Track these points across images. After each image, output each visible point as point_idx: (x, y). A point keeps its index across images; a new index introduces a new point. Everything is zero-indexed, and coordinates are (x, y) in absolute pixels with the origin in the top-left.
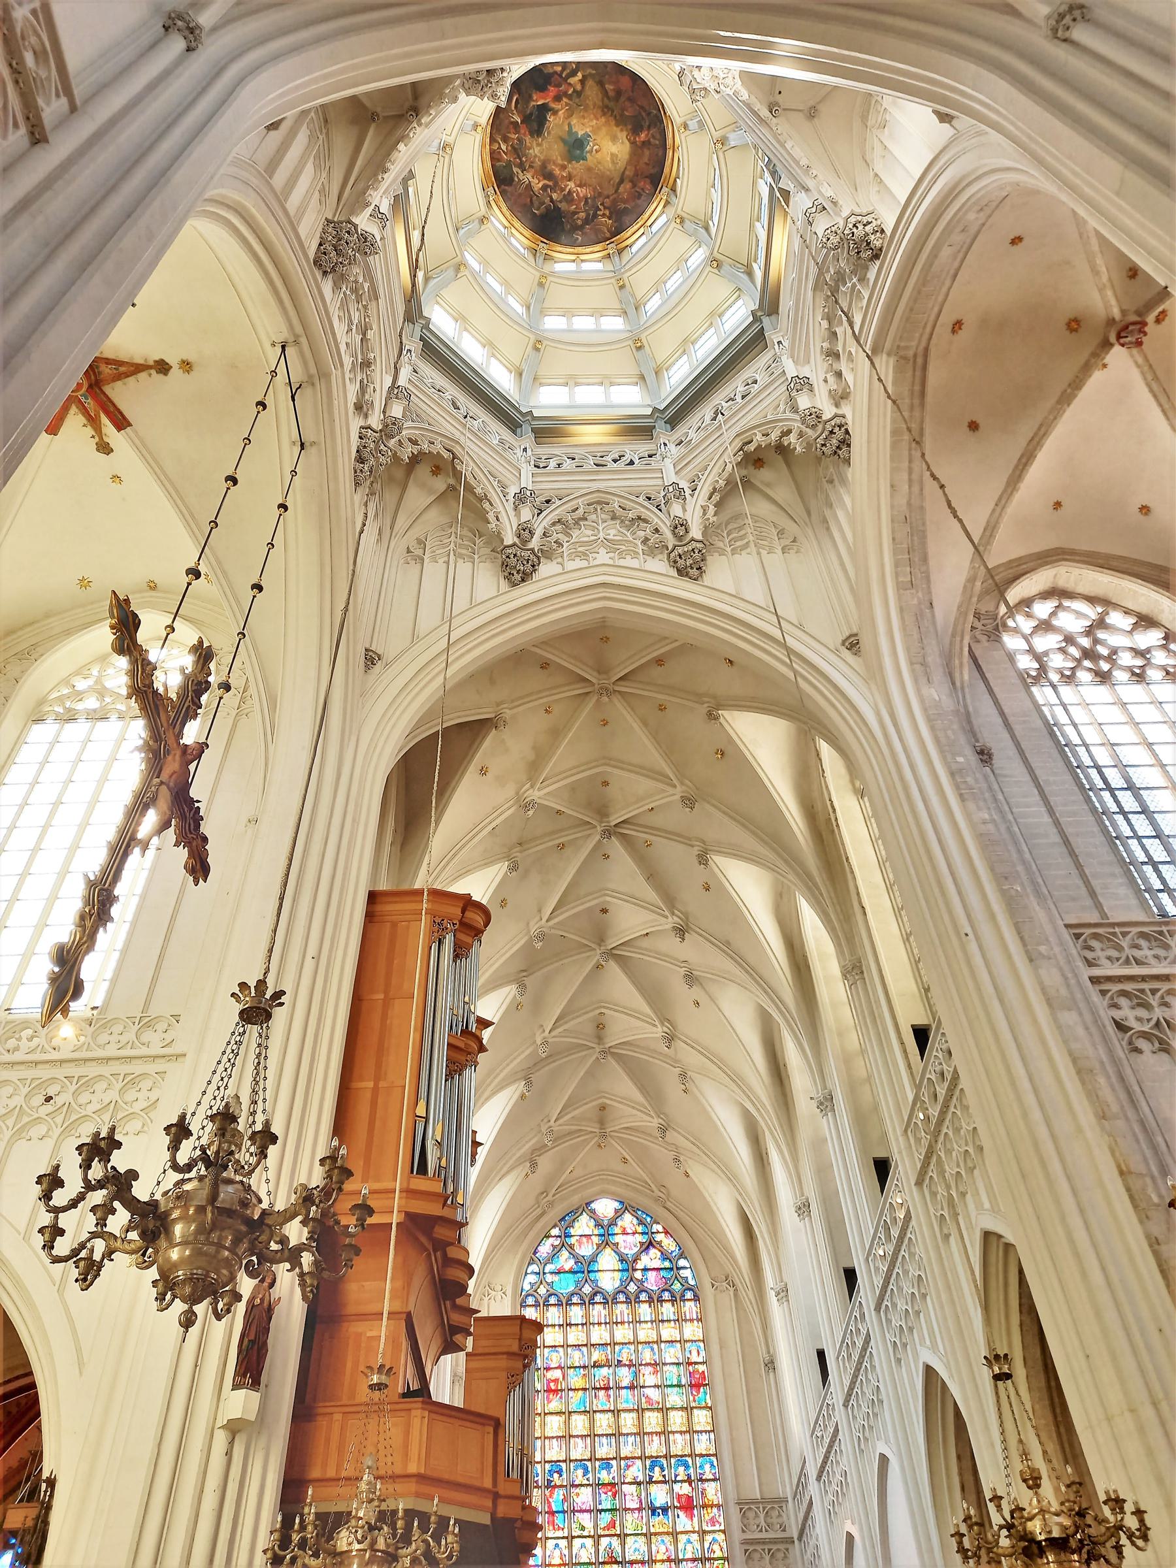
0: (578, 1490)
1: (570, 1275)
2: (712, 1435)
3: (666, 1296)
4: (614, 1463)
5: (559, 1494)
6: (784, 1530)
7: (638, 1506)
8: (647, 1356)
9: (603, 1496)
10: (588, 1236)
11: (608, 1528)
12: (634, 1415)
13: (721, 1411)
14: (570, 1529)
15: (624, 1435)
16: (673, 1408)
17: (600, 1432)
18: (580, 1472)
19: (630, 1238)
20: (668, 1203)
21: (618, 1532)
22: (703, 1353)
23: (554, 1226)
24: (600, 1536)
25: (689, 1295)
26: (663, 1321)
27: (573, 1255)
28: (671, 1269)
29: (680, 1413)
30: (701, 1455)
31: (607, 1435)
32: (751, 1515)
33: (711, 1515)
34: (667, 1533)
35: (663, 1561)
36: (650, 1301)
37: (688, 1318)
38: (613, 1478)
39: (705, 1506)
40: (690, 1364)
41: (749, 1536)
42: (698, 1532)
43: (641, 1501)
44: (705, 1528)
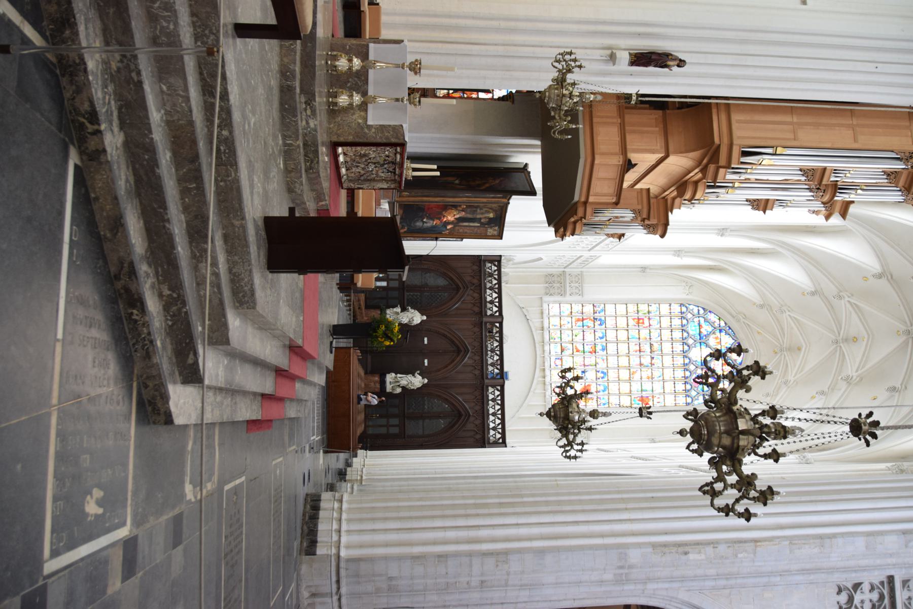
1: (698, 332)
5: (591, 324)
18: (601, 335)
23: (726, 323)
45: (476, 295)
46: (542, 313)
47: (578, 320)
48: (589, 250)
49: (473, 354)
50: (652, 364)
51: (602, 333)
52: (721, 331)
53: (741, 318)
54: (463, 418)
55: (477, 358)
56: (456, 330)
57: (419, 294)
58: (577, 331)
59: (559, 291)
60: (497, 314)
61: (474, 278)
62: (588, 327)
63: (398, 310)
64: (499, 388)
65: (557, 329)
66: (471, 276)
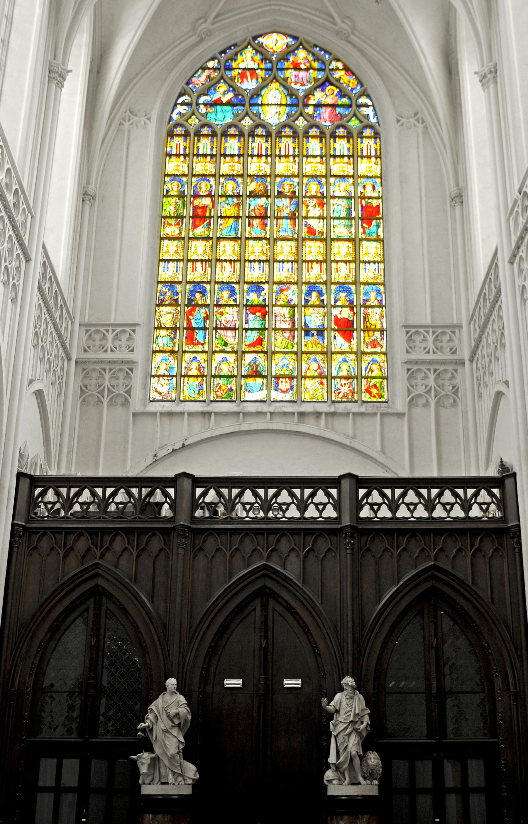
0: (222, 310)
1: (229, 108)
2: (381, 266)
3: (341, 132)
4: (266, 286)
5: (201, 313)
6: (455, 353)
7: (290, 326)
8: (313, 188)
9: (251, 316)
10: (253, 71)
11: (253, 345)
12: (293, 244)
13: (395, 243)
14: (211, 343)
15: (279, 261)
16: (339, 239)
17: (252, 258)
18: (226, 294)
19: (302, 74)
20: (352, 37)
21: (265, 350)
22: (379, 188)
23: (213, 59)
24: (244, 352)
25: (368, 132)
26: (335, 156)
27: (232, 88)
28: (349, 106)
29: (347, 244)
30: (367, 284)
31: (259, 261)
32: (418, 339)
33: (373, 338)
34: (322, 353)
35: (313, 377)
36: (322, 136)
37: (365, 154)
38: (264, 300)
39: (367, 330)
40: (364, 198)
41: (414, 356)
42: (356, 353)
43: (293, 323)
44: (364, 349)
45: (119, 544)
46: (170, 414)
47: (191, 339)
48: (28, 260)
49: (274, 554)
50: (293, 196)
51: (221, 290)
52: (230, 69)
53: (204, 26)
54: (440, 586)
55: (284, 546)
56: (209, 596)
57: (103, 701)
58: (215, 342)
59: (121, 375)
60: (171, 491)
61: (71, 548)
62: (206, 318)
63: (145, 757)
64: (362, 492)
65: (209, 385)
66: (65, 556)
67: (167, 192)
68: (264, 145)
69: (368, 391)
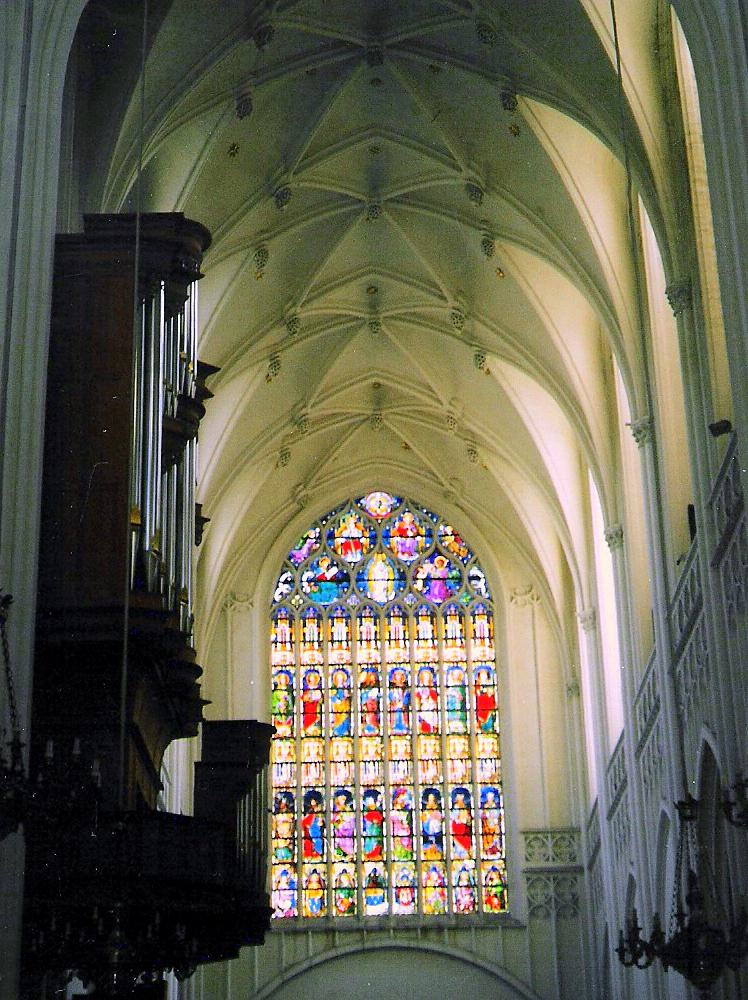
9: (368, 823)
19: (409, 542)
41: (533, 865)
43: (412, 832)
44: (483, 856)
67: (276, 685)
68: (374, 629)
69: (489, 901)
